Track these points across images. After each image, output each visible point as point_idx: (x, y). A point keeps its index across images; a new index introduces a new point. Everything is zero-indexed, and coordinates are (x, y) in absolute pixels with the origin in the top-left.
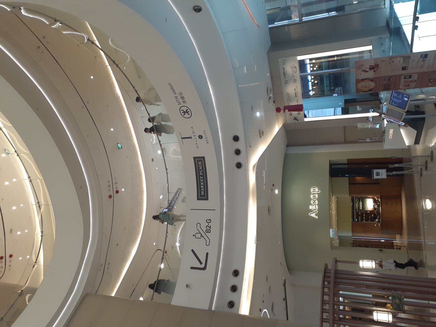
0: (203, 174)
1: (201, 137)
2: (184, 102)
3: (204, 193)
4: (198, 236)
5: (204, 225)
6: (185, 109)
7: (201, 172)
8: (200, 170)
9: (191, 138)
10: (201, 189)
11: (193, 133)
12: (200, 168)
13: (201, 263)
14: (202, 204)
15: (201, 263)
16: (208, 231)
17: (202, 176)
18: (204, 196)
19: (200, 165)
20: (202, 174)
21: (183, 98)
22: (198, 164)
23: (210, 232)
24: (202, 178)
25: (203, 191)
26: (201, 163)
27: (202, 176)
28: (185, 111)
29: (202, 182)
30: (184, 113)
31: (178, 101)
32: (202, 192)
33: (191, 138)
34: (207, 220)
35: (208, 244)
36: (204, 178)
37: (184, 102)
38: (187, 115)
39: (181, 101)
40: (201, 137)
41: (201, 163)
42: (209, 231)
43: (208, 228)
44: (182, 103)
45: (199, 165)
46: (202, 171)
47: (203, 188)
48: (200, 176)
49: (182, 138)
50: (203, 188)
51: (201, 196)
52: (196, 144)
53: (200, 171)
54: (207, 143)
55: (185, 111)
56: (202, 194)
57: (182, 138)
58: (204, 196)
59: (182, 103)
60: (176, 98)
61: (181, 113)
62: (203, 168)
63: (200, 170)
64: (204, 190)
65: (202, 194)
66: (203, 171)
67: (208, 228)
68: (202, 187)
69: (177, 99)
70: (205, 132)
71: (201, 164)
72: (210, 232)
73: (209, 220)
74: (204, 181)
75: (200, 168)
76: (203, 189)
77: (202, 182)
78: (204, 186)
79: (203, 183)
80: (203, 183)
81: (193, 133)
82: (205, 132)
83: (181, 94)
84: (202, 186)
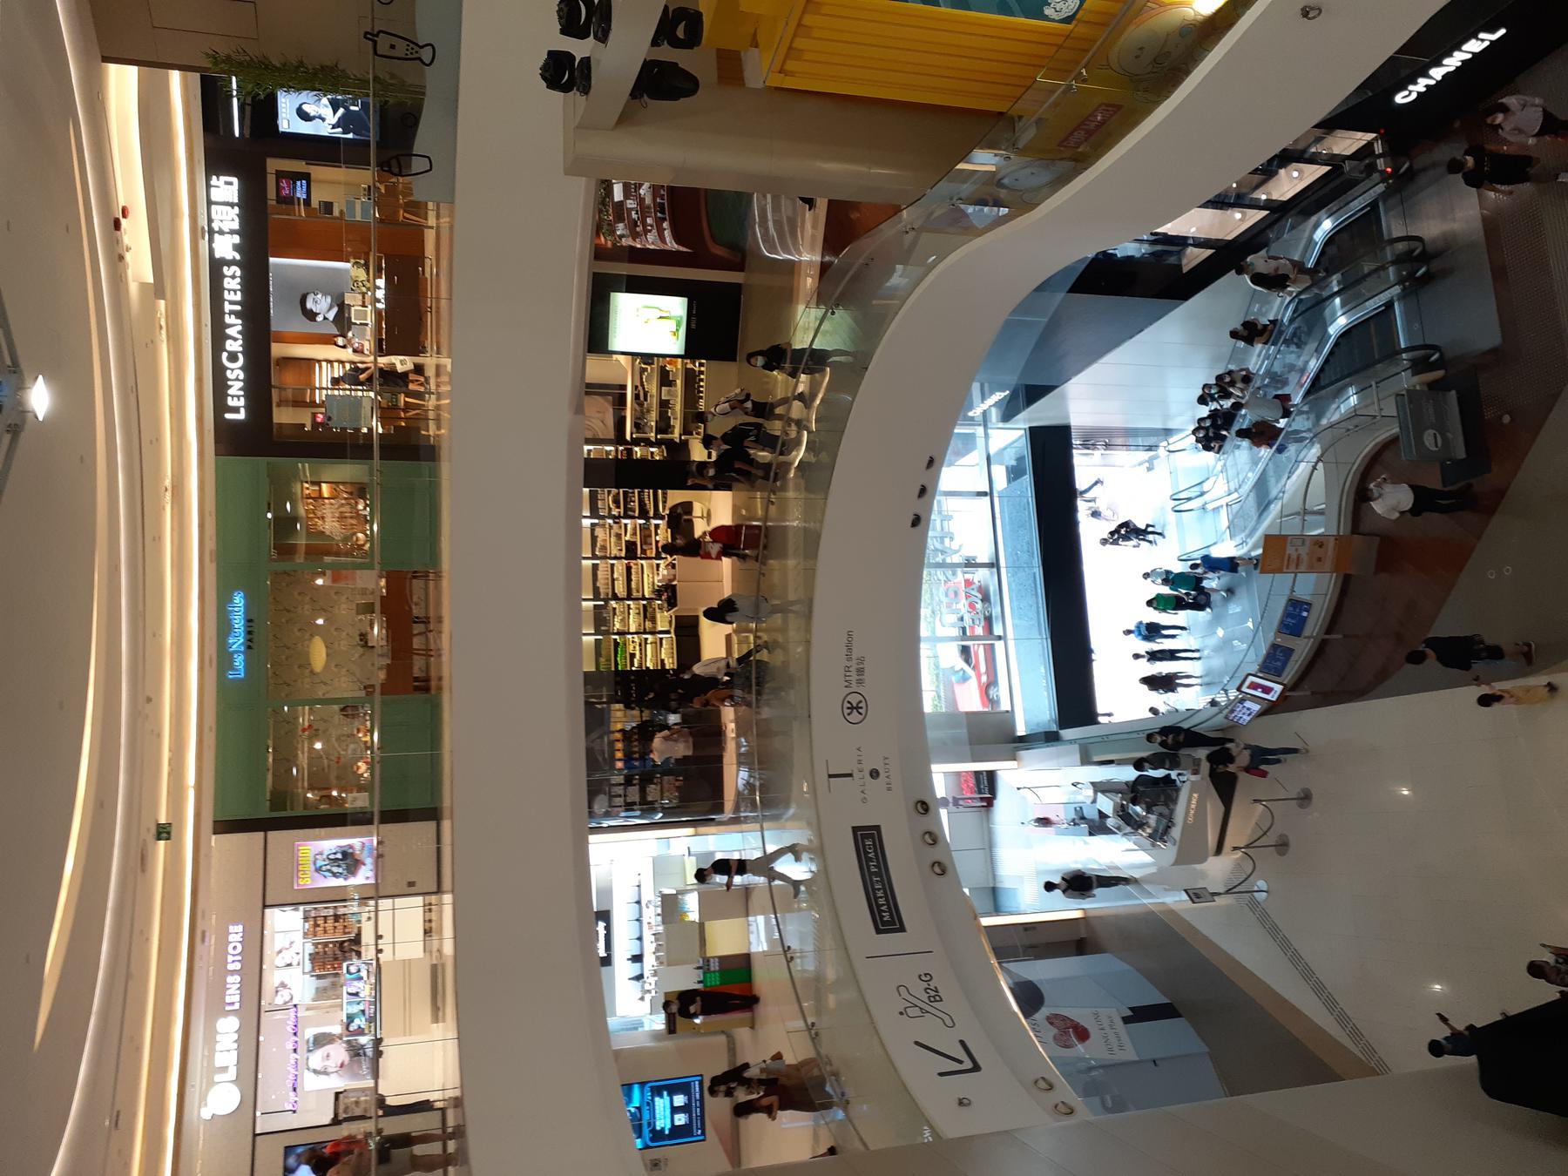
1: (874, 774)
2: (860, 682)
3: (891, 916)
4: (916, 1012)
5: (918, 989)
6: (854, 699)
8: (871, 860)
9: (850, 775)
10: (879, 906)
11: (860, 762)
13: (960, 1062)
14: (891, 941)
15: (960, 1062)
16: (935, 997)
17: (876, 874)
18: (892, 923)
21: (860, 671)
22: (864, 846)
23: (941, 1000)
25: (885, 912)
27: (876, 874)
28: (855, 705)
29: (879, 889)
30: (849, 711)
31: (847, 678)
33: (850, 775)
34: (920, 976)
35: (949, 1023)
36: (881, 877)
37: (860, 682)
38: (855, 717)
39: (854, 677)
40: (874, 774)
42: (938, 998)
43: (933, 993)
44: (854, 683)
49: (830, 776)
51: (884, 923)
52: (862, 792)
54: (889, 789)
55: (855, 705)
57: (830, 776)
58: (892, 923)
59: (854, 683)
60: (847, 669)
61: (845, 710)
62: (876, 855)
63: (871, 860)
64: (889, 908)
66: (878, 861)
67: (933, 993)
68: (881, 901)
69: (848, 674)
70: (887, 761)
72: (941, 1000)
73: (926, 975)
74: (883, 885)
78: (887, 900)
81: (860, 762)
82: (887, 761)
83: (861, 660)
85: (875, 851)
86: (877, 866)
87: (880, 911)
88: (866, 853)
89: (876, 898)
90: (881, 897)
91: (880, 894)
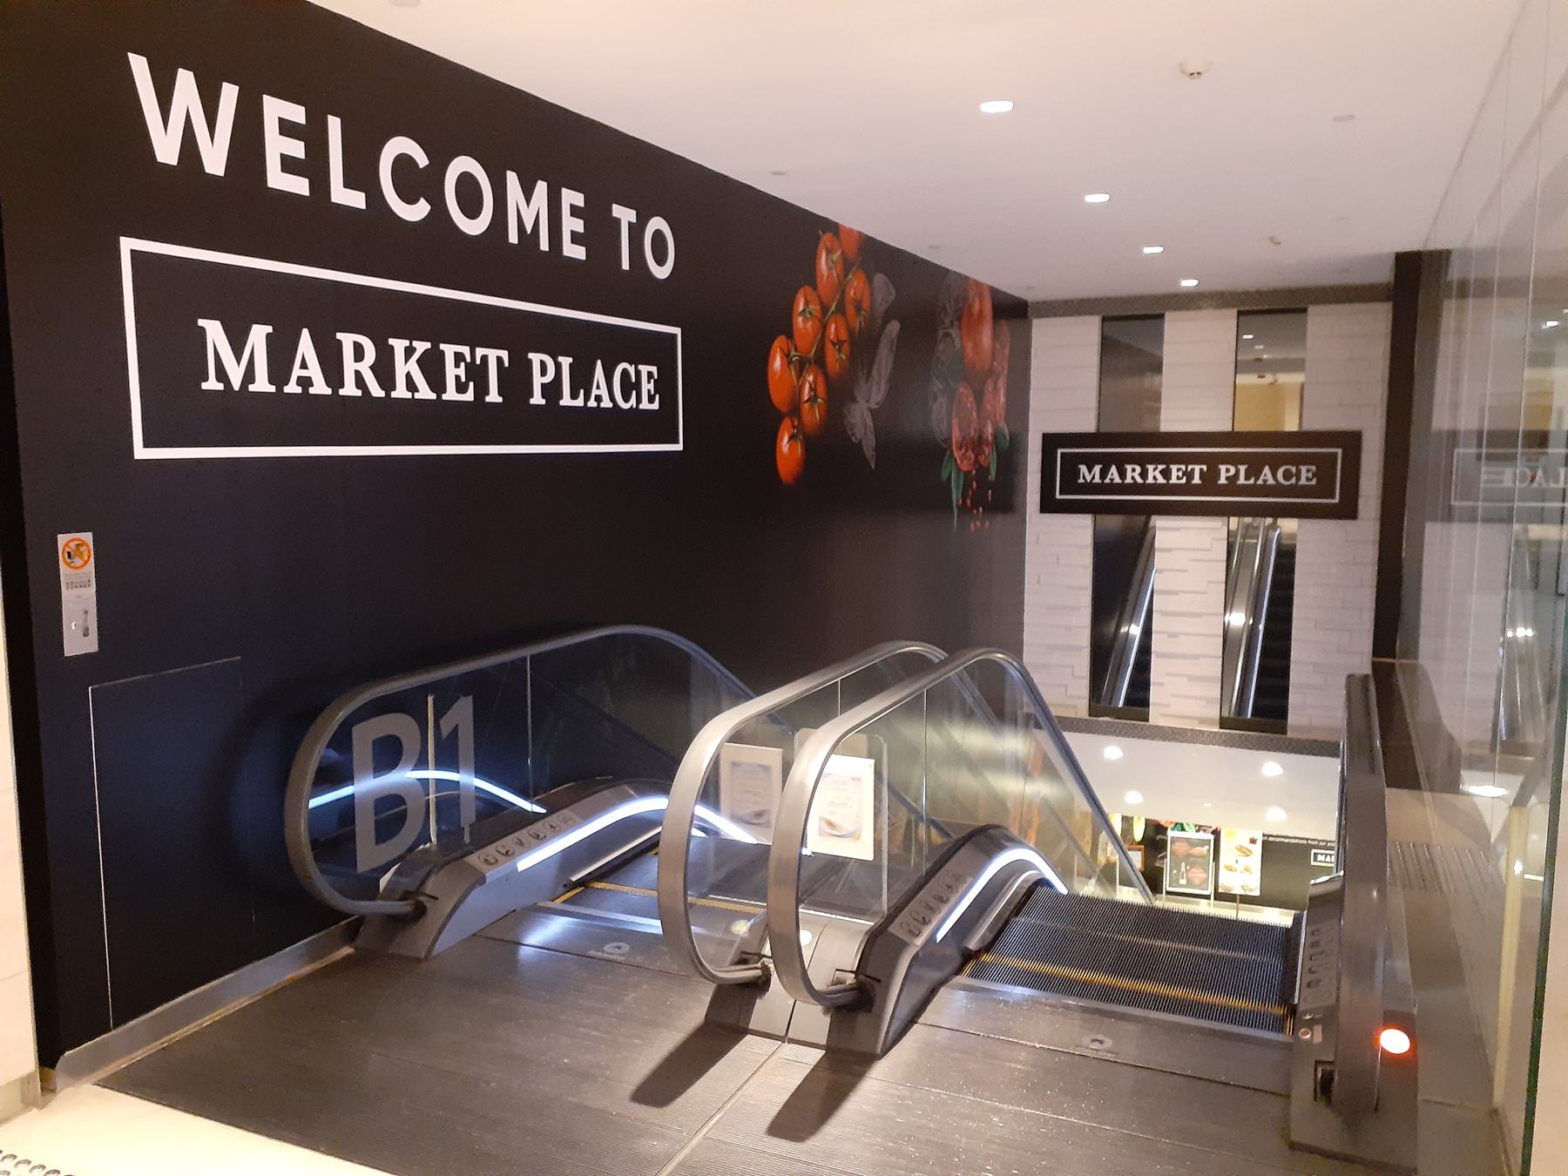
0: (1223, 491)
7: (1238, 471)
8: (1253, 472)
10: (1121, 462)
12: (1267, 470)
17: (1210, 478)
18: (1071, 484)
19: (1287, 475)
20: (1223, 481)
22: (1298, 460)
24: (1197, 480)
25: (1103, 474)
26: (1303, 481)
27: (1210, 478)
29: (1166, 474)
32: (1097, 469)
41: (1303, 481)
45: (1294, 469)
46: (1242, 481)
47: (1122, 474)
48: (1213, 462)
50: (1122, 474)
51: (1071, 464)
53: (1242, 468)
56: (1083, 468)
62: (1265, 490)
63: (1253, 472)
65: (1083, 468)
71: (1298, 479)
75: (1267, 470)
76: (1117, 480)
77: (1166, 474)
79: (1161, 480)
80: (1161, 480)
84: (1138, 469)
85: (1277, 490)
86: (1232, 487)
87: (1106, 462)
88: (1275, 462)
89: (1143, 461)
90: (1144, 474)
91: (1154, 474)
